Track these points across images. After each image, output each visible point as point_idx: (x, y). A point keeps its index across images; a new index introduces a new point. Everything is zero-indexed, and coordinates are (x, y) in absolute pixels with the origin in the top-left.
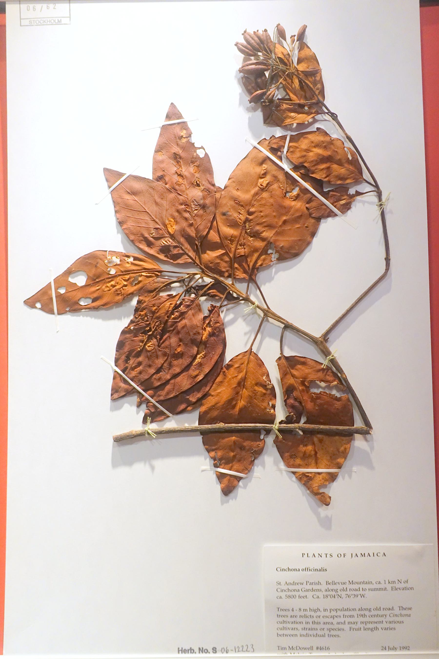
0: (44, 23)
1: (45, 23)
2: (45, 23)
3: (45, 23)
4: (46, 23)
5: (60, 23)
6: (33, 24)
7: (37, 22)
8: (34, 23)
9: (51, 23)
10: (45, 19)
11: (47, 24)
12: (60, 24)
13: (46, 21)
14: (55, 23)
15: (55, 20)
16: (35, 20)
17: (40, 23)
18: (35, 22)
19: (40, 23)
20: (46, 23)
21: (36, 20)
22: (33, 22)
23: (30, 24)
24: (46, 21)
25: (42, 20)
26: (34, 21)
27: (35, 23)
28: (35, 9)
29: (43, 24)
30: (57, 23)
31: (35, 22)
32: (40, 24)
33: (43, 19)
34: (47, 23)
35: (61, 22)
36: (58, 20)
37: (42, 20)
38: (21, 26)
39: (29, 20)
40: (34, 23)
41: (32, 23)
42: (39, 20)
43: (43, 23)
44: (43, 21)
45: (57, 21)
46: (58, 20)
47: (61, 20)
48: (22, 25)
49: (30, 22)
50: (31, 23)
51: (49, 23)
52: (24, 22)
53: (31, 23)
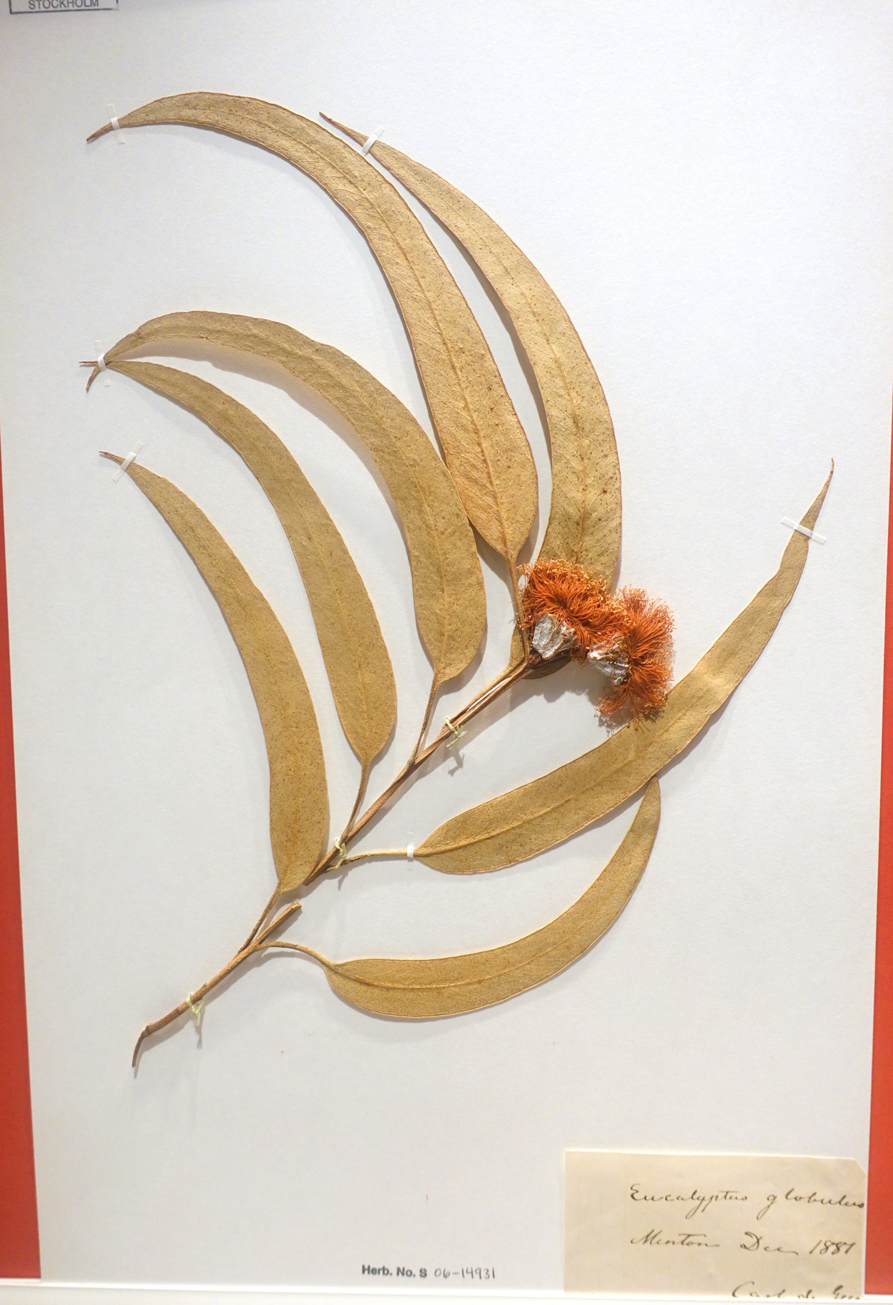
0: (61, 7)
1: (63, 8)
2: (62, 6)
3: (62, 6)
4: (65, 7)
5: (96, 7)
6: (37, 9)
8: (39, 7)
9: (76, 8)
11: (67, 8)
12: (95, 10)
14: (85, 6)
19: (51, 7)
23: (30, 7)
27: (41, 6)
29: (59, 9)
30: (89, 6)
32: (51, 9)
34: (68, 6)
35: (98, 5)
38: (11, 13)
40: (39, 7)
41: (35, 6)
43: (58, 5)
48: (13, 11)
51: (71, 7)
53: (32, 7)
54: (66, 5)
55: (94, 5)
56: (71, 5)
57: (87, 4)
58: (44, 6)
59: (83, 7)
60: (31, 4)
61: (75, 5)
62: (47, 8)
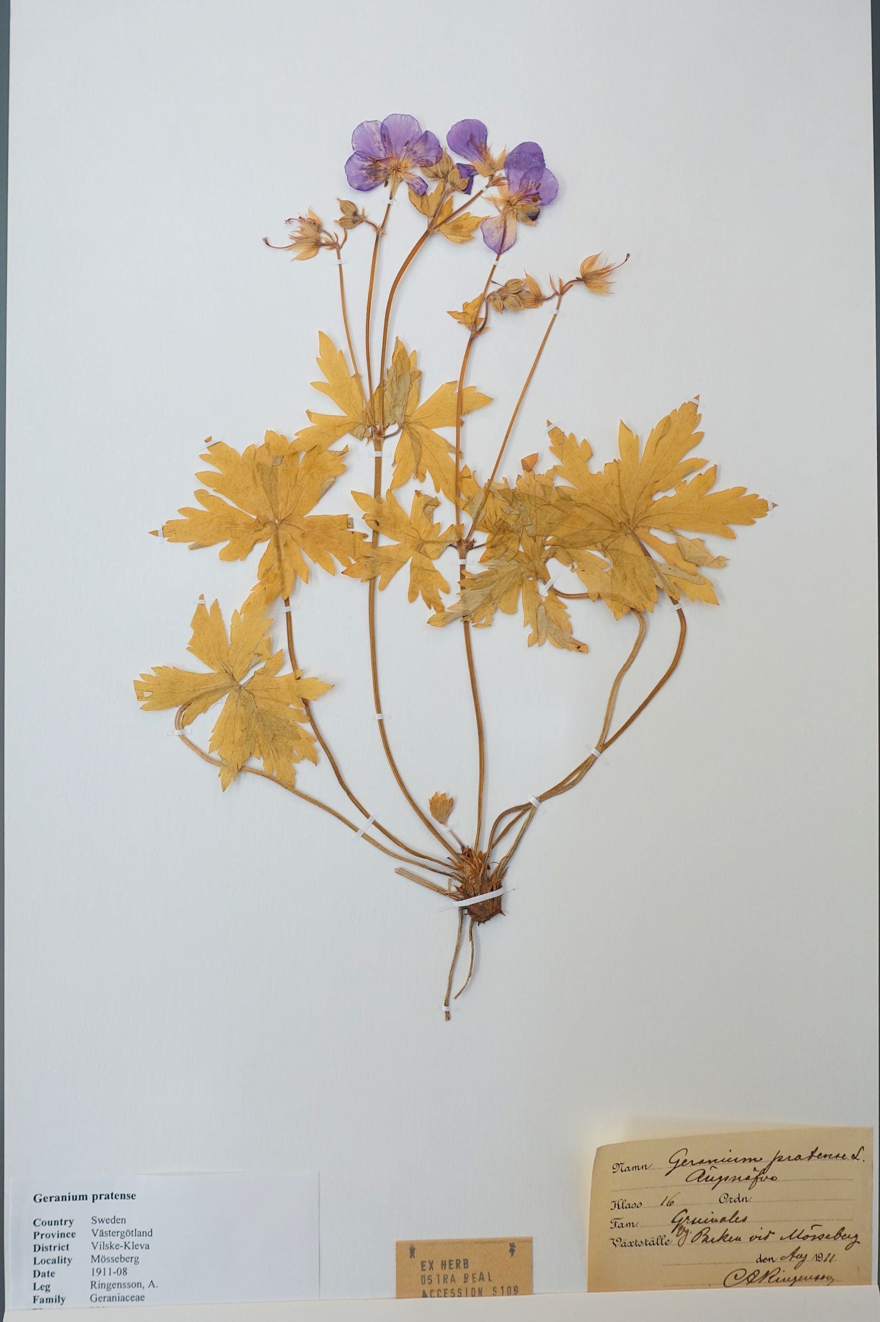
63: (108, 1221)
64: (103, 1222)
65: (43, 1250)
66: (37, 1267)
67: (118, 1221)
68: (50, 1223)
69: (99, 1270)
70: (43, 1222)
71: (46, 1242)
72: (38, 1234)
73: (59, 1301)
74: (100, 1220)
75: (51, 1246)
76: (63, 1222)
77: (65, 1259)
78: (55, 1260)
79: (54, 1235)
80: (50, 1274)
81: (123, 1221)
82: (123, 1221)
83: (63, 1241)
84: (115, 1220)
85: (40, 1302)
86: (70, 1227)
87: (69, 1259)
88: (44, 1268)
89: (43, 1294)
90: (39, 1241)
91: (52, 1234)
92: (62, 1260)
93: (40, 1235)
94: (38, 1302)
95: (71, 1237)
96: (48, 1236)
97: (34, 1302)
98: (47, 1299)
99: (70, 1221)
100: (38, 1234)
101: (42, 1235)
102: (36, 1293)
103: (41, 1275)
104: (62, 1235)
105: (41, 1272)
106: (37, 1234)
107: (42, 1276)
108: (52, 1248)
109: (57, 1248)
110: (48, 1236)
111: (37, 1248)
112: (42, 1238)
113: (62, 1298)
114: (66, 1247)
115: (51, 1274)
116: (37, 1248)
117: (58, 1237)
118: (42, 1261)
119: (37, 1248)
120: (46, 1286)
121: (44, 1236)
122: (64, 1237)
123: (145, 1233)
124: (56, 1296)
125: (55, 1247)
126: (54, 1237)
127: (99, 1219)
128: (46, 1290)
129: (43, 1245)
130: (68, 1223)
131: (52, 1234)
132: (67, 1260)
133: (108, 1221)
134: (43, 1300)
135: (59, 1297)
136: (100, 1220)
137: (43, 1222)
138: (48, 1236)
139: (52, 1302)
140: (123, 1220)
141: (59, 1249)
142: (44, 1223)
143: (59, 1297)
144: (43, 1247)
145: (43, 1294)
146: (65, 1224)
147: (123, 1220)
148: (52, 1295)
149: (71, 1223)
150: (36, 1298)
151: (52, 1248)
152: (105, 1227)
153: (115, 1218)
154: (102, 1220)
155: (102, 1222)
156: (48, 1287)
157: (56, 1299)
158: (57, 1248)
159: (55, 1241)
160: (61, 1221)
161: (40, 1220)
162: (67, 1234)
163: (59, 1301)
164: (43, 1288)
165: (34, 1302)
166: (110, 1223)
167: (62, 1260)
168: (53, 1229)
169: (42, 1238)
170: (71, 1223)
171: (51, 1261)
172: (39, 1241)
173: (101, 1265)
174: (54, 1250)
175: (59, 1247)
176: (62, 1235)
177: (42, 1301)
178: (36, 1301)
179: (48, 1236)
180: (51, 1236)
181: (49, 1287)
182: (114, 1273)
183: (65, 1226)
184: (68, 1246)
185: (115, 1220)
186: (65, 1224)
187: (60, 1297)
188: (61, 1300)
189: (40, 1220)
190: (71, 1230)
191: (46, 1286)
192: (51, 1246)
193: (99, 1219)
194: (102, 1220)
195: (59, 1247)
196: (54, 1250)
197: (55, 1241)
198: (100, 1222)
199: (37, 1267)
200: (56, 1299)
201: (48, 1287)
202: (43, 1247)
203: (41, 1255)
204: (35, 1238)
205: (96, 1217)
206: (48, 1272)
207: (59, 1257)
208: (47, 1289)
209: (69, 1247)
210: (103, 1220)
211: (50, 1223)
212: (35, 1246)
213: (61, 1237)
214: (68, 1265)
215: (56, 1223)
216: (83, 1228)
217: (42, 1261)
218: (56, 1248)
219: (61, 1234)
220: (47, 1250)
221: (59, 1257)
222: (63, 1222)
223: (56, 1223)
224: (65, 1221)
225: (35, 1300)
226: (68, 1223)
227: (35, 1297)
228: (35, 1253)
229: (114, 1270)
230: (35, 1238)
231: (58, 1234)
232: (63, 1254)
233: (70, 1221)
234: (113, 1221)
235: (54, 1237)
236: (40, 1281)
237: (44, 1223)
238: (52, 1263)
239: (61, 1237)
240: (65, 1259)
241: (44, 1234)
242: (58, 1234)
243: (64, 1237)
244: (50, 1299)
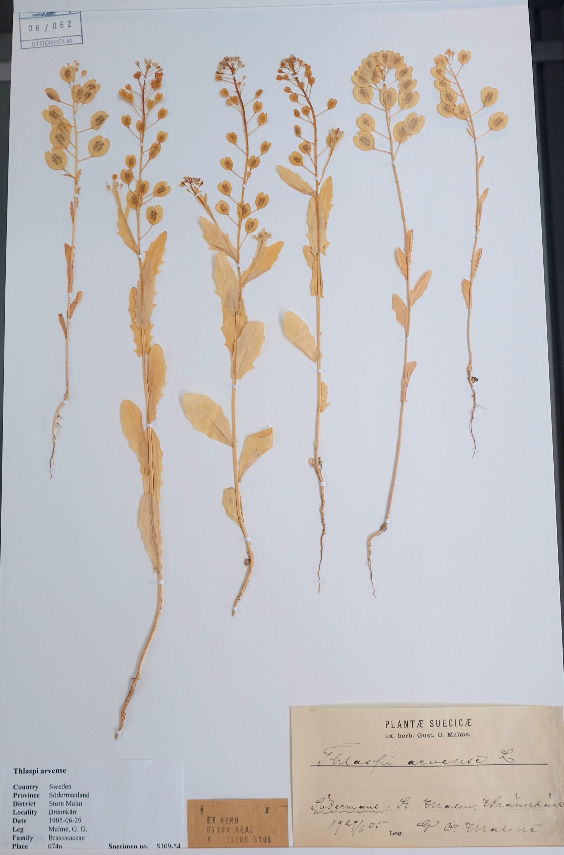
1: (51, 45)
2: (51, 43)
4: (53, 44)
5: (70, 43)
6: (36, 46)
7: (42, 43)
8: (38, 45)
9: (59, 44)
10: (51, 40)
11: (54, 45)
13: (53, 42)
15: (64, 40)
16: (39, 42)
17: (46, 44)
18: (39, 43)
19: (45, 44)
20: (53, 44)
21: (40, 41)
22: (36, 44)
23: (32, 46)
24: (53, 42)
25: (48, 41)
26: (37, 42)
28: (39, 28)
29: (49, 45)
30: (66, 43)
31: (39, 43)
32: (45, 45)
33: (48, 40)
35: (71, 42)
36: (67, 40)
37: (48, 41)
38: (22, 48)
39: (32, 41)
40: (38, 45)
42: (44, 40)
44: (49, 43)
45: (66, 41)
46: (67, 40)
47: (71, 39)
48: (23, 48)
49: (32, 44)
50: (33, 45)
51: (56, 44)
52: (25, 45)
53: (33, 45)
54: (53, 43)
55: (69, 42)
56: (56, 43)
57: (65, 42)
58: (40, 44)
59: (63, 44)
60: (34, 44)
61: (58, 43)
62: (43, 45)
63: (60, 788)
64: (57, 788)
65: (19, 805)
66: (15, 816)
67: (67, 787)
68: (24, 788)
69: (54, 820)
70: (19, 787)
71: (21, 800)
72: (16, 794)
73: (29, 839)
74: (55, 787)
75: (24, 803)
76: (32, 787)
77: (33, 811)
78: (26, 812)
79: (26, 795)
80: (23, 821)
81: (70, 787)
82: (70, 787)
83: (32, 800)
84: (65, 787)
85: (17, 839)
86: (36, 790)
87: (35, 812)
88: (19, 817)
89: (19, 834)
90: (17, 799)
91: (25, 795)
92: (31, 812)
93: (17, 795)
94: (15, 839)
95: (37, 797)
96: (22, 796)
97: (13, 839)
98: (21, 838)
99: (36, 786)
100: (16, 794)
101: (19, 795)
102: (14, 833)
103: (18, 822)
104: (31, 796)
105: (18, 820)
106: (15, 794)
107: (18, 822)
108: (25, 804)
109: (28, 804)
110: (22, 796)
111: (16, 804)
112: (18, 797)
113: (31, 837)
114: (33, 804)
115: (24, 821)
116: (16, 804)
117: (29, 797)
118: (18, 812)
119: (16, 804)
120: (21, 829)
121: (20, 796)
122: (32, 797)
123: (84, 795)
124: (27, 836)
125: (26, 804)
126: (26, 797)
127: (54, 786)
128: (21, 832)
129: (19, 802)
130: (35, 788)
131: (25, 795)
132: (34, 812)
133: (60, 788)
134: (19, 838)
135: (29, 836)
136: (55, 787)
137: (19, 787)
138: (22, 796)
139: (25, 839)
140: (70, 787)
141: (29, 805)
142: (20, 788)
143: (29, 836)
144: (19, 804)
145: (19, 834)
146: (33, 788)
147: (70, 787)
148: (24, 835)
149: (37, 788)
150: (15, 837)
151: (25, 804)
152: (57, 791)
153: (64, 786)
154: (56, 786)
155: (56, 788)
156: (22, 829)
157: (27, 838)
158: (28, 804)
159: (26, 800)
160: (31, 786)
161: (18, 785)
162: (34, 795)
163: (29, 839)
164: (19, 830)
165: (13, 839)
166: (61, 788)
167: (31, 812)
168: (26, 792)
169: (18, 797)
170: (37, 788)
171: (24, 813)
172: (17, 799)
173: (56, 816)
174: (26, 805)
175: (29, 803)
176: (31, 796)
177: (18, 839)
178: (14, 839)
179: (22, 796)
180: (24, 796)
181: (23, 829)
182: (64, 821)
183: (33, 790)
184: (34, 803)
185: (65, 787)
186: (33, 788)
187: (30, 836)
188: (30, 838)
189: (18, 785)
190: (37, 793)
191: (21, 829)
192: (24, 803)
193: (54, 786)
194: (56, 786)
195: (29, 803)
196: (26, 805)
197: (26, 800)
198: (55, 788)
199: (15, 816)
200: (27, 838)
201: (22, 829)
202: (19, 804)
203: (18, 809)
204: (14, 797)
205: (52, 785)
206: (22, 820)
207: (29, 810)
208: (22, 831)
209: (35, 804)
210: (57, 786)
211: (24, 788)
212: (14, 802)
213: (31, 797)
214: (34, 816)
215: (28, 787)
216: (44, 792)
217: (18, 812)
218: (27, 804)
219: (31, 795)
220: (22, 805)
221: (29, 810)
222: (32, 787)
223: (28, 787)
224: (33, 787)
225: (14, 838)
226: (35, 788)
227: (14, 836)
228: (14, 807)
229: (64, 819)
230: (14, 797)
231: (29, 795)
232: (31, 808)
233: (36, 786)
234: (63, 787)
235: (26, 797)
236: (17, 826)
237: (20, 788)
238: (25, 814)
239: (31, 797)
240: (33, 811)
241: (20, 795)
242: (29, 795)
243: (32, 797)
244: (23, 838)
